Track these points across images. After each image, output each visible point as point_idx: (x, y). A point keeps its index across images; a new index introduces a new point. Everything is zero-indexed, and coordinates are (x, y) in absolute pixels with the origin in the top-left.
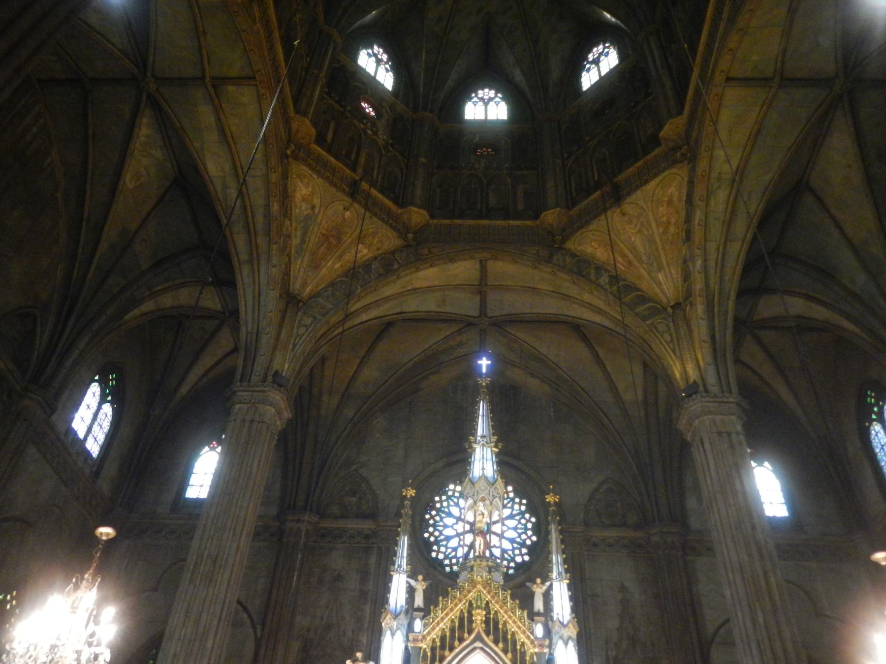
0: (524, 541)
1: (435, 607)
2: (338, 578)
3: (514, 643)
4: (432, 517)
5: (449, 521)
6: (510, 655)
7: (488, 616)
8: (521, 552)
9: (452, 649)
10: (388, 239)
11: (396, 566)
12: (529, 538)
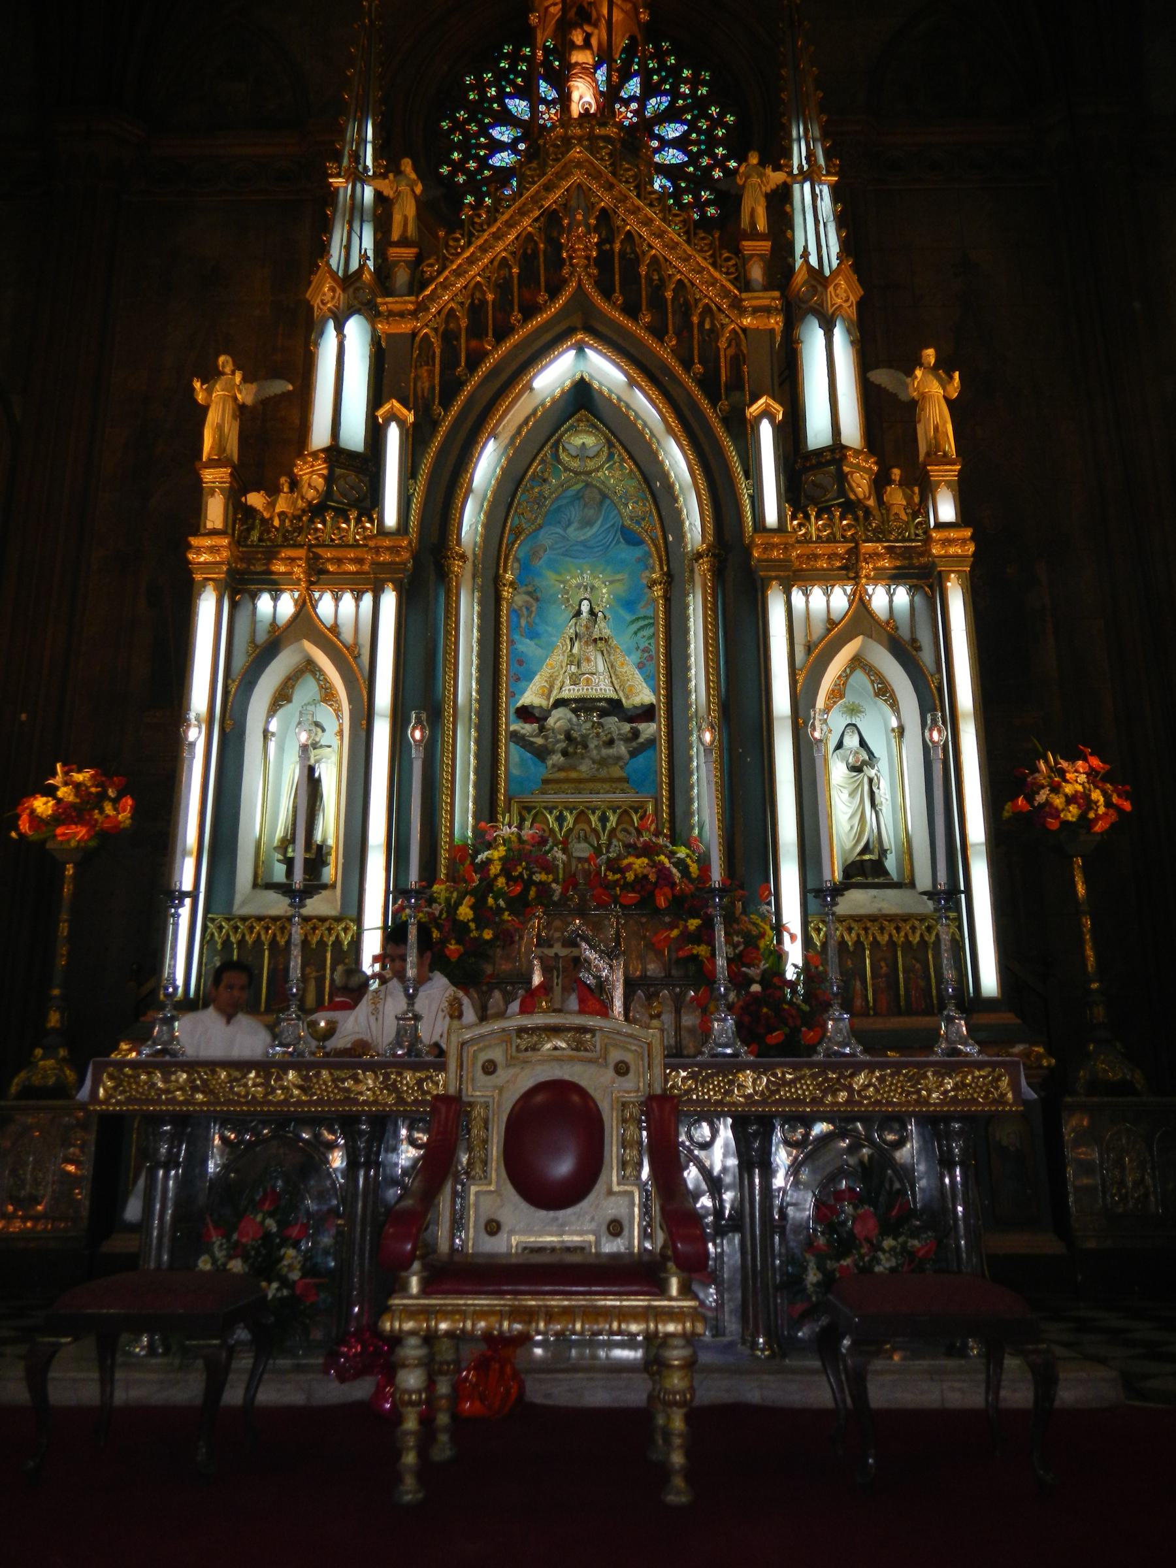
0: (710, 168)
1: (451, 231)
3: (685, 310)
4: (458, 126)
5: (503, 134)
7: (608, 246)
8: (697, 197)
9: (502, 335)
11: (345, 162)
12: (721, 163)
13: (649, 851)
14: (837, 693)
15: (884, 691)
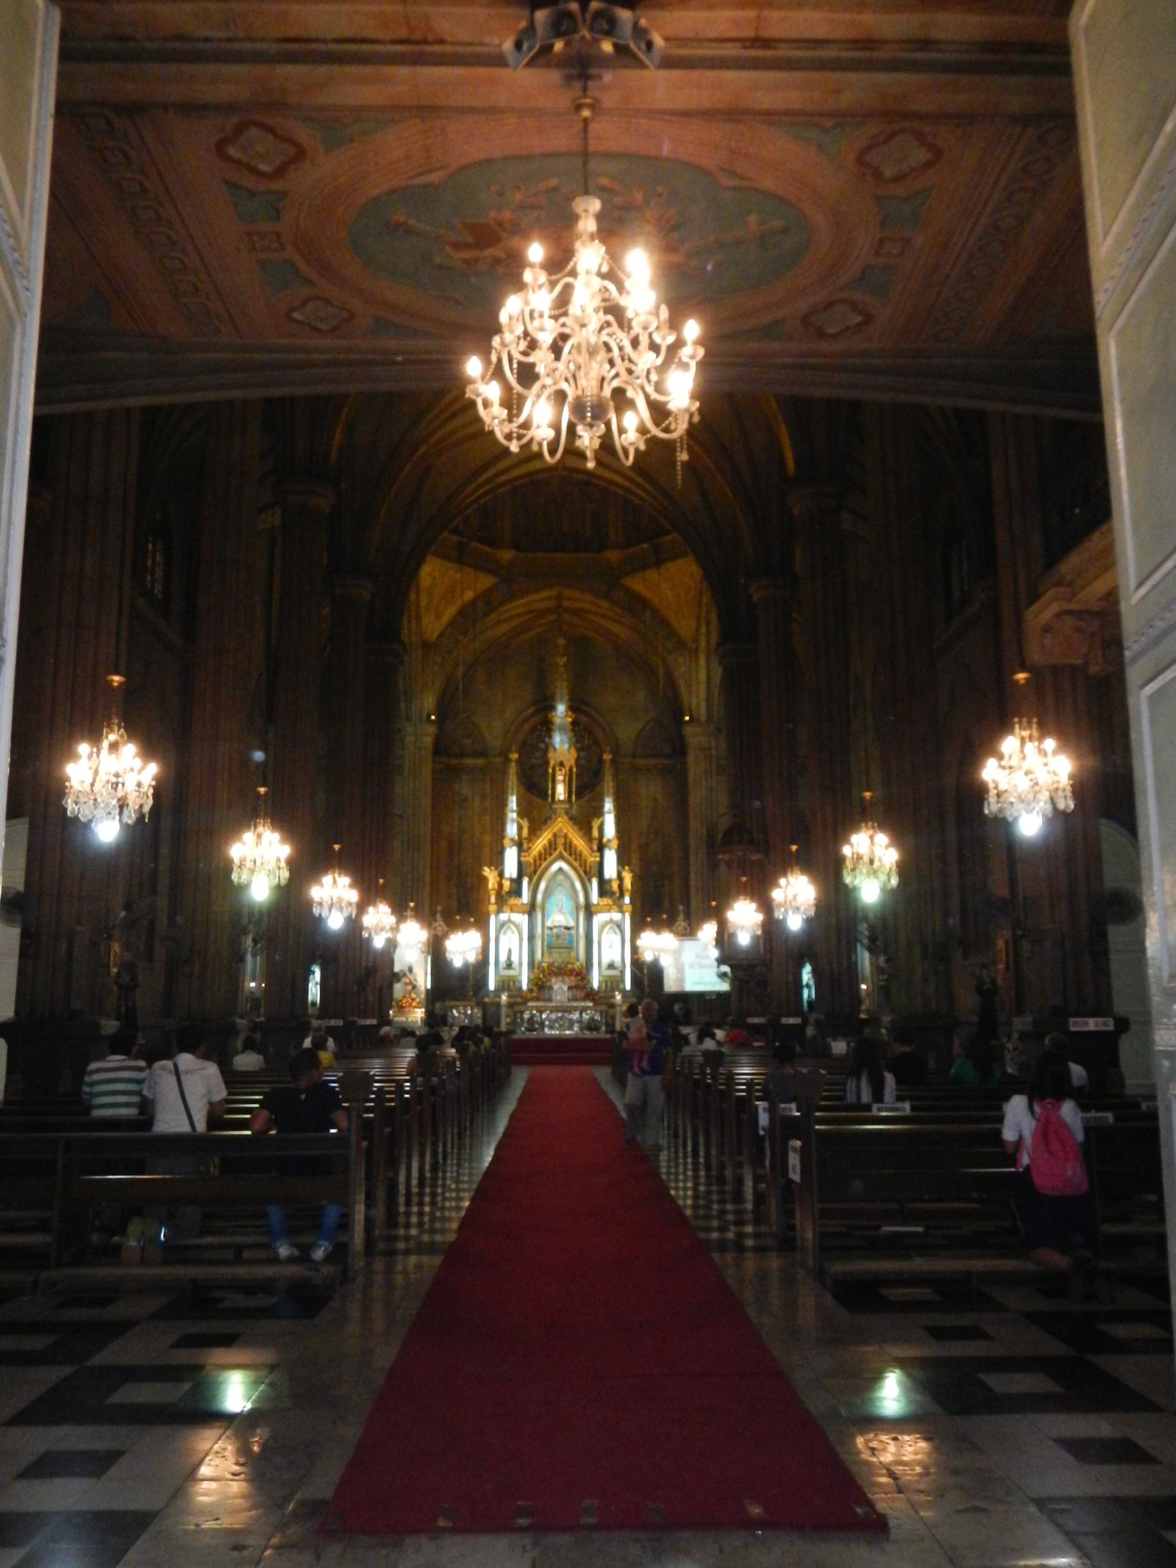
2: (465, 800)
3: (581, 855)
6: (578, 862)
9: (545, 859)
10: (487, 581)
13: (572, 964)
14: (607, 933)
15: (615, 933)
